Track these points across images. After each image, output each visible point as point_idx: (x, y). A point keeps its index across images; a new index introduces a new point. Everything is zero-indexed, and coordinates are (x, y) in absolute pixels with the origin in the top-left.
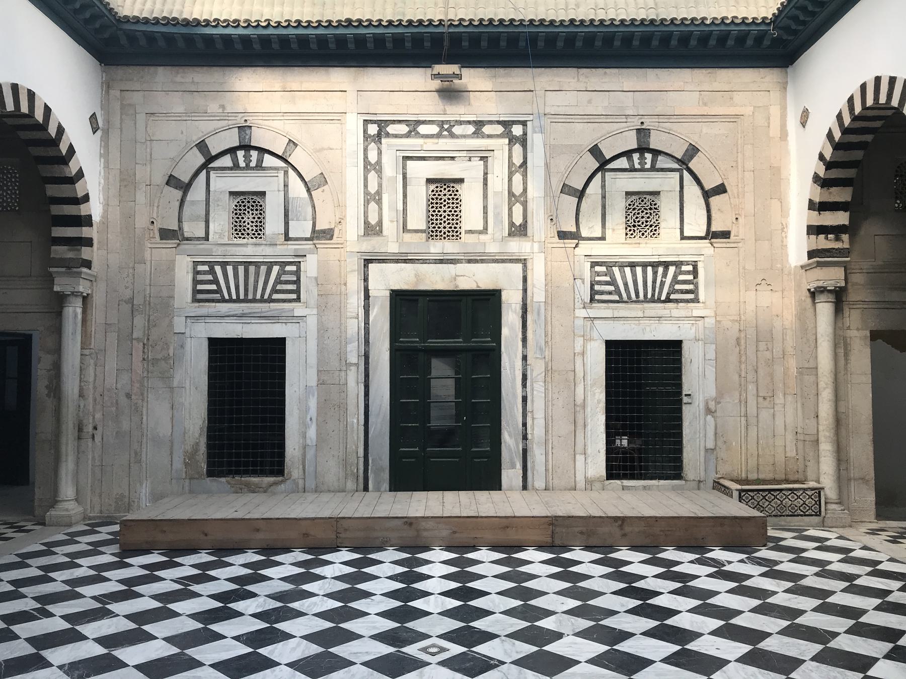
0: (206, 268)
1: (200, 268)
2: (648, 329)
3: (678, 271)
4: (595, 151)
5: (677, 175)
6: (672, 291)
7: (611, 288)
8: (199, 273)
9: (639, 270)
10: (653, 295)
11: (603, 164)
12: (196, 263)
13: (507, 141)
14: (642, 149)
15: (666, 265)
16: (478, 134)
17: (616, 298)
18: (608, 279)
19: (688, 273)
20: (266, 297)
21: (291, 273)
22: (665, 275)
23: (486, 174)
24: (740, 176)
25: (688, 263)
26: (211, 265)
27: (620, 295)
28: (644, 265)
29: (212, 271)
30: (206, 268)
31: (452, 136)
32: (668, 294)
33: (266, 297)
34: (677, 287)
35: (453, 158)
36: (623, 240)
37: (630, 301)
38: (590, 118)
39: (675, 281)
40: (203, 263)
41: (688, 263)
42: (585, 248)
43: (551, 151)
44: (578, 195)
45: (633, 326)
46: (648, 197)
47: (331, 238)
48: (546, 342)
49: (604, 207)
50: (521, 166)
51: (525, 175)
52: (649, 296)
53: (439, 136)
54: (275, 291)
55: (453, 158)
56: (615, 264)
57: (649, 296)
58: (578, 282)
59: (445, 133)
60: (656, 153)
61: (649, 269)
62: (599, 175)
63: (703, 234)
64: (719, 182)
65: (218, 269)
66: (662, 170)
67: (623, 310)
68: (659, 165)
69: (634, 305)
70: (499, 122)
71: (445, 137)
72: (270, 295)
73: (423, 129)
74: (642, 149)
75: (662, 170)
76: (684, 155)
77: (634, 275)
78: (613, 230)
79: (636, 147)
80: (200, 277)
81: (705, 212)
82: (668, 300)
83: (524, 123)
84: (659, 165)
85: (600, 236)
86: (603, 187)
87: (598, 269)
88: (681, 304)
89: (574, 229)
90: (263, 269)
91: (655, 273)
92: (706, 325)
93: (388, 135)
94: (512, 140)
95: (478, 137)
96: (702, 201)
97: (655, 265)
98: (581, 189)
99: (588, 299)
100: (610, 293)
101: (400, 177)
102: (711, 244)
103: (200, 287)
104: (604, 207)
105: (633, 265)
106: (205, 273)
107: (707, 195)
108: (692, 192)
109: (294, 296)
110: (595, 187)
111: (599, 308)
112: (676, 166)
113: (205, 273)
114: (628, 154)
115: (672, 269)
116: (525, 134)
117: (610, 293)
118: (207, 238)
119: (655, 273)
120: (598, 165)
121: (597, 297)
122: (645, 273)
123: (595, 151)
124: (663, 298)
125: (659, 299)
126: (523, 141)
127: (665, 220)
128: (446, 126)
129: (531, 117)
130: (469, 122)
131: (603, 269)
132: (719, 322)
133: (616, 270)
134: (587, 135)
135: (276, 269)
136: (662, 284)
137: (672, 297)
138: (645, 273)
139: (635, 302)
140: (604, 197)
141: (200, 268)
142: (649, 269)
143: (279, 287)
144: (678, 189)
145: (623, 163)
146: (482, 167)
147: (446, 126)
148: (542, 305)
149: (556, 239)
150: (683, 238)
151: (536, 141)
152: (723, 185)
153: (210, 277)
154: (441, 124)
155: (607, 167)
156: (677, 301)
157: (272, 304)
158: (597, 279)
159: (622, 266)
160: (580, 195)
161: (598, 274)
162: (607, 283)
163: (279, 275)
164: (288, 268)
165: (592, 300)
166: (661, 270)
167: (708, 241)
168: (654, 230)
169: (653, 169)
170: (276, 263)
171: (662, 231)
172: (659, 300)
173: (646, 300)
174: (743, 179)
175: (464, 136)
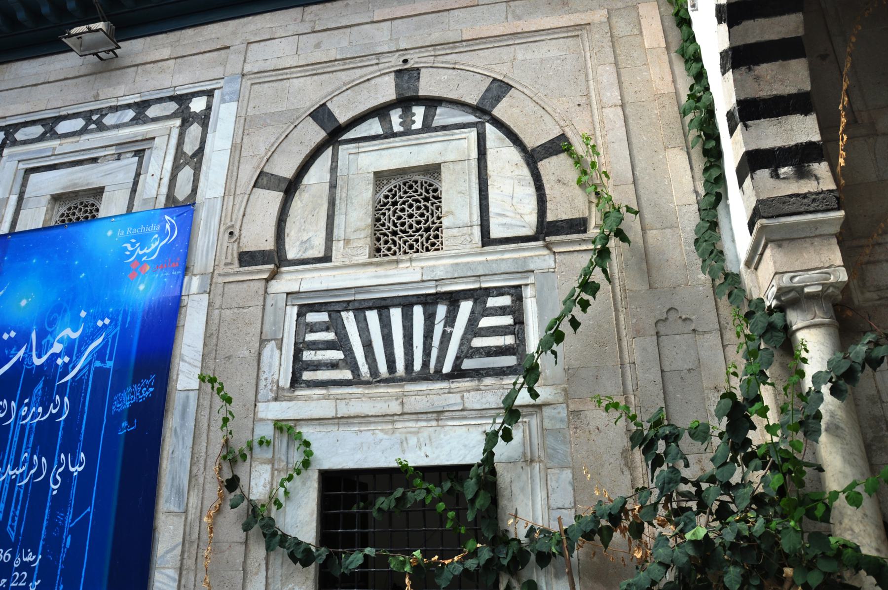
2: (413, 441)
3: (479, 308)
4: (321, 114)
5: (473, 134)
6: (466, 352)
7: (337, 355)
9: (396, 314)
10: (426, 364)
11: (335, 134)
13: (178, 122)
14: (405, 102)
15: (453, 299)
16: (140, 118)
17: (347, 375)
18: (330, 336)
19: (502, 311)
22: (450, 320)
23: (138, 175)
24: (597, 118)
25: (500, 292)
27: (355, 369)
28: (407, 304)
31: (102, 128)
32: (458, 359)
34: (477, 342)
35: (95, 160)
36: (364, 258)
37: (375, 379)
38: (315, 69)
39: (473, 329)
41: (500, 292)
42: (289, 281)
43: (246, 124)
44: (284, 186)
45: (380, 435)
46: (420, 178)
48: (192, 477)
49: (332, 204)
50: (194, 155)
51: (197, 169)
52: (417, 366)
53: (83, 131)
55: (95, 160)
56: (347, 306)
57: (417, 366)
58: (271, 346)
59: (93, 126)
60: (432, 103)
61: (418, 312)
62: (329, 151)
63: (530, 231)
64: (555, 133)
67: (359, 401)
68: (438, 121)
69: (382, 390)
70: (171, 98)
71: (92, 131)
73: (63, 127)
74: (405, 102)
75: (444, 128)
76: (483, 98)
77: (386, 325)
78: (347, 241)
79: (394, 97)
81: (531, 190)
82: (458, 373)
83: (210, 94)
84: (438, 121)
86: (334, 169)
88: (488, 381)
91: (430, 319)
92: (547, 424)
93: (15, 143)
94: (187, 119)
95: (137, 124)
96: (525, 172)
97: (429, 302)
99: (285, 381)
100: (333, 365)
101: (14, 199)
102: (547, 246)
104: (332, 204)
105: (383, 307)
107: (532, 158)
108: (504, 158)
110: (318, 174)
111: (308, 398)
112: (472, 119)
114: (381, 112)
115: (466, 308)
116: (209, 107)
117: (333, 365)
119: (430, 319)
120: (322, 134)
121: (307, 376)
122: (408, 319)
123: (321, 114)
124: (447, 368)
125: (438, 371)
126: (204, 119)
127: (450, 213)
128: (95, 118)
129: (221, 83)
130: (129, 106)
131: (323, 317)
132: (576, 413)
133: (349, 319)
134: (309, 92)
136: (446, 338)
137: (468, 364)
138: (408, 319)
139: (386, 381)
140: (333, 186)
144: (474, 154)
145: (374, 127)
146: (135, 166)
147: (95, 118)
148: (193, 396)
149: (236, 267)
150: (487, 240)
151: (225, 116)
152: (563, 137)
154: (87, 116)
155: (344, 137)
156: (478, 374)
158: (310, 337)
159: (360, 309)
160: (290, 188)
161: (313, 328)
162: (329, 345)
165: (296, 381)
166: (441, 311)
167: (540, 243)
168: (430, 237)
169: (427, 127)
171: (445, 234)
172: (439, 376)
173: (411, 376)
174: (601, 121)
175: (117, 126)
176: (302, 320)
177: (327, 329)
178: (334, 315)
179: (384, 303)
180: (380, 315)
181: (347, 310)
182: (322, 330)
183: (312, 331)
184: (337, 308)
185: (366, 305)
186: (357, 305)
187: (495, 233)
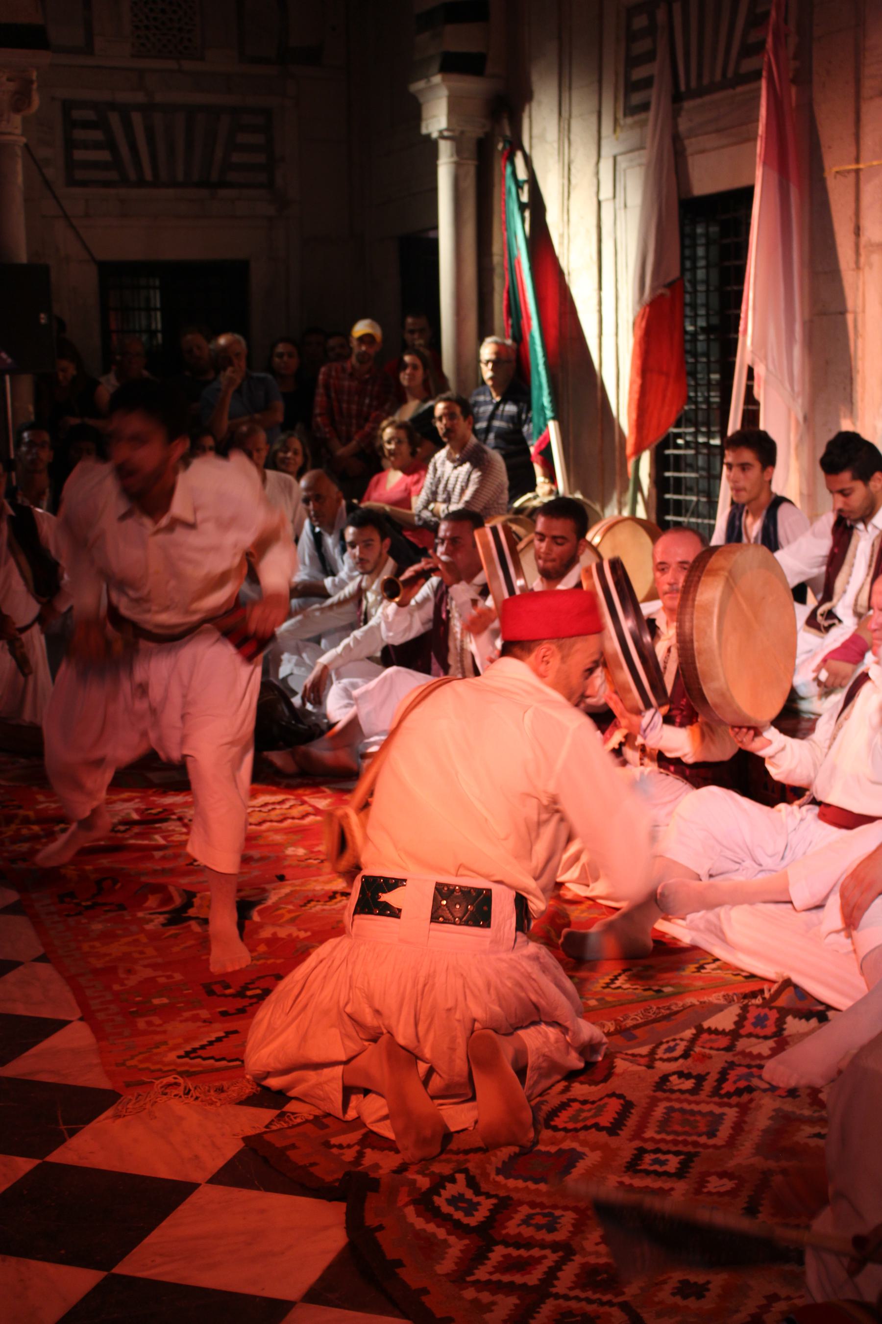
157: (739, 89)
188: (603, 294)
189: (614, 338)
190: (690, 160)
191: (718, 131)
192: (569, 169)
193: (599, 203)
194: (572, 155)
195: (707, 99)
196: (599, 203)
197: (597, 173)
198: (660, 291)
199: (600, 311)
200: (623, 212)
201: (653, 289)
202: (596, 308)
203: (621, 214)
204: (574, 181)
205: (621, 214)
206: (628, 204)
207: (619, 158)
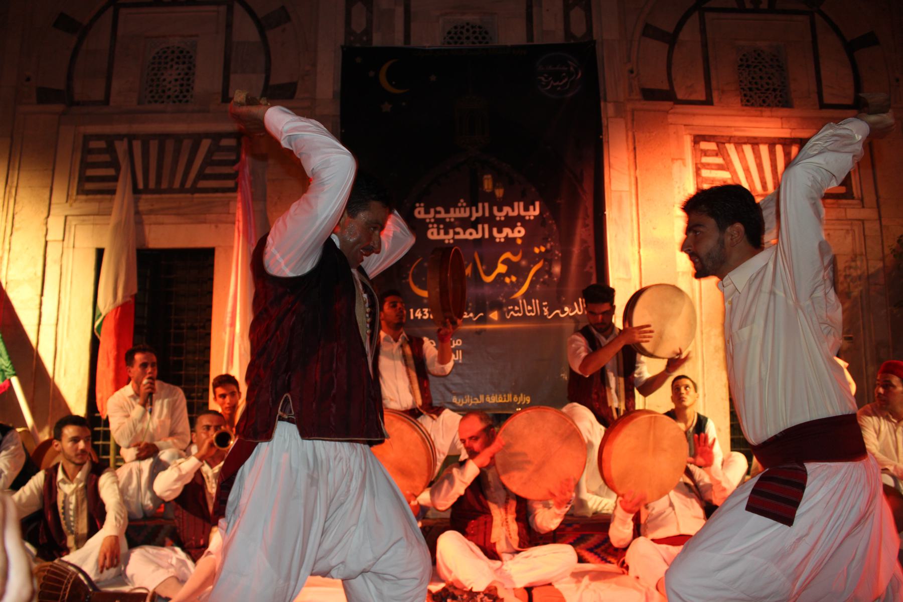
0: (102, 144)
1: (94, 145)
8: (90, 151)
12: (87, 138)
20: (188, 185)
21: (228, 149)
26: (110, 139)
29: (111, 149)
30: (102, 144)
33: (188, 185)
40: (99, 137)
47: (294, 93)
54: (201, 176)
56: (730, 139)
65: (121, 147)
66: (784, 12)
72: (195, 182)
80: (92, 158)
85: (704, 98)
87: (704, 145)
89: (665, 87)
90: (187, 144)
98: (671, 31)
103: (90, 172)
106: (100, 151)
107: (851, 48)
109: (230, 184)
113: (100, 151)
118: (106, 102)
135: (206, 144)
138: (772, 153)
141: (94, 145)
142: (779, 149)
143: (208, 171)
153: (106, 158)
157: (196, 195)
163: (210, 152)
164: (225, 142)
170: (207, 135)
176: (697, 146)
177: (717, 155)
178: (720, 145)
179: (755, 141)
180: (753, 149)
181: (730, 143)
182: (713, 156)
183: (706, 155)
184: (723, 141)
185: (743, 141)
186: (736, 140)
187: (828, 100)
188: (44, 298)
189: (54, 327)
190: (147, 229)
191: (178, 214)
192: (13, 218)
193: (46, 242)
194: (17, 210)
195: (164, 196)
196: (46, 242)
197: (47, 223)
198: (128, 299)
199: (40, 308)
200: (71, 250)
201: (124, 297)
202: (38, 306)
203: (69, 253)
204: (16, 225)
205: (69, 253)
206: (76, 246)
207: (69, 218)
